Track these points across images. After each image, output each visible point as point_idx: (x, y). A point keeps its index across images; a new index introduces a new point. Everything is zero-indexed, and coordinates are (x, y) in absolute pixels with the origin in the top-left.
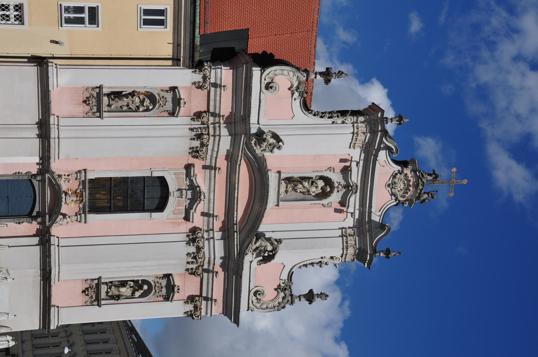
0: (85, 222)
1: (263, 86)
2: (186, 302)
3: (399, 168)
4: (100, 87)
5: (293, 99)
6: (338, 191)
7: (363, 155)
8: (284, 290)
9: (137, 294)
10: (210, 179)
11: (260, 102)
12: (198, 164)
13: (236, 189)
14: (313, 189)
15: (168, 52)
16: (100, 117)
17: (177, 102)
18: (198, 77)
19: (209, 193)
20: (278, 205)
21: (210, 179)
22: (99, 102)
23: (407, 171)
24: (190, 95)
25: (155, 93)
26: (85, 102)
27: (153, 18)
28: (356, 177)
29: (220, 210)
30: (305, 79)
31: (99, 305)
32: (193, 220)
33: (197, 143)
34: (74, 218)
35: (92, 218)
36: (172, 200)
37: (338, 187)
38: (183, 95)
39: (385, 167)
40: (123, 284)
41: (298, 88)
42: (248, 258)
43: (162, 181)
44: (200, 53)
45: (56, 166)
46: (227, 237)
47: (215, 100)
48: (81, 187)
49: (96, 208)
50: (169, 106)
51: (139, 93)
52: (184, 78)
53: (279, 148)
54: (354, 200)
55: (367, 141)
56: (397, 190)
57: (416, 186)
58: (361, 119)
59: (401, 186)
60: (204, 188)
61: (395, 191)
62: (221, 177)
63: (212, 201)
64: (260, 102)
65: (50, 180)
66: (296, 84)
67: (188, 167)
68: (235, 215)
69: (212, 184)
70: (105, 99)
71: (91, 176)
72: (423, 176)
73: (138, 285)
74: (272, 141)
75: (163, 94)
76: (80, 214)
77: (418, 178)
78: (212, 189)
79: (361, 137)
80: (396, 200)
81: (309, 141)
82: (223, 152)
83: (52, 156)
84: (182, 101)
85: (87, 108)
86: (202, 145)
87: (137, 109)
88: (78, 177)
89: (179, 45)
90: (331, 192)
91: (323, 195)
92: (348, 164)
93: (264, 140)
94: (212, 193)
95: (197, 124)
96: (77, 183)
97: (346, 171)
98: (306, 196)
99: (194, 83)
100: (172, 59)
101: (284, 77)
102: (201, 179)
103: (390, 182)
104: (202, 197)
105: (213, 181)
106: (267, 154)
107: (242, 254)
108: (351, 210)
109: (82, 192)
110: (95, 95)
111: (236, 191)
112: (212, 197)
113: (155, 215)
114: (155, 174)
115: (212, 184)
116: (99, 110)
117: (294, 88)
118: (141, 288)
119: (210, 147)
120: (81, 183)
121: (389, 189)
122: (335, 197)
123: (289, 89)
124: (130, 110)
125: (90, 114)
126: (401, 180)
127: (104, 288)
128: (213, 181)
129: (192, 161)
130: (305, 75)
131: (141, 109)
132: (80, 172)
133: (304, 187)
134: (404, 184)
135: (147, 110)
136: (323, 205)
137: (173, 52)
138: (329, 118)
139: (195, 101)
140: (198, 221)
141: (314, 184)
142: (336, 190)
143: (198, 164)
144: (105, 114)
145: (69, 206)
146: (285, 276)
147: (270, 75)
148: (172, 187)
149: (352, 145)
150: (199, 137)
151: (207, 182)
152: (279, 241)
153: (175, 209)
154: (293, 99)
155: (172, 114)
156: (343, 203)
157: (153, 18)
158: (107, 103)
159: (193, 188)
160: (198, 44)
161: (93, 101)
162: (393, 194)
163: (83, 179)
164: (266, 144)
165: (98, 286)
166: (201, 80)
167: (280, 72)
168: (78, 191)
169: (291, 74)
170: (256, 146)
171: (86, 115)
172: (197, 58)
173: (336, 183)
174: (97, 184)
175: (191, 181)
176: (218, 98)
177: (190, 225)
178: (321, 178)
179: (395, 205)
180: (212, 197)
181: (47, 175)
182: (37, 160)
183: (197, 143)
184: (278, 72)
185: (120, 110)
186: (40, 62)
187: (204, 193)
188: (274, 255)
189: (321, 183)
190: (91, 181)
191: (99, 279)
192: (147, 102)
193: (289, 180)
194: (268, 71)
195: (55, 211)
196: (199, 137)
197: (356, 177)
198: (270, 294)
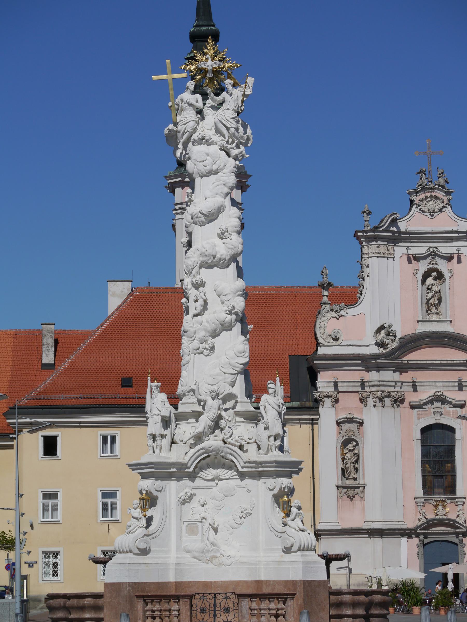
0: (465, 498)
1: (335, 343)
3: (414, 207)
4: (338, 487)
5: (347, 315)
6: (437, 264)
7: (400, 244)
10: (424, 386)
11: (350, 346)
12: (412, 397)
13: (432, 362)
15: (306, 428)
16: (364, 487)
17: (350, 420)
18: (328, 402)
19: (437, 386)
20: (451, 321)
21: (424, 386)
22: (351, 489)
23: (417, 199)
26: (351, 500)
29: (453, 376)
30: (328, 306)
32: (462, 401)
33: (388, 401)
34: (460, 507)
35: (459, 492)
36: (444, 421)
37: (433, 265)
38: (343, 415)
39: (414, 222)
41: (336, 312)
43: (424, 431)
44: (307, 401)
45: (411, 524)
47: (348, 386)
48: (431, 501)
49: (451, 489)
50: (354, 427)
51: (342, 454)
52: (328, 415)
53: (390, 326)
54: (445, 248)
55: (386, 243)
56: (436, 208)
57: (432, 189)
58: (365, 250)
59: (431, 205)
61: (437, 209)
63: (445, 384)
64: (350, 346)
65: (424, 528)
66: (333, 314)
68: (458, 362)
69: (428, 384)
71: (419, 492)
72: (421, 185)
74: (383, 333)
75: (343, 433)
76: (457, 502)
77: (424, 189)
78: (433, 384)
79: (383, 249)
80: (446, 207)
81: (388, 296)
82: (396, 376)
83: (399, 527)
84: (348, 416)
86: (389, 396)
87: (358, 455)
88: (422, 504)
89: (300, 420)
92: (411, 256)
93: (382, 341)
94: (437, 384)
95: (370, 401)
96: (427, 505)
97: (417, 258)
99: (333, 406)
100: (312, 425)
101: (327, 325)
102: (424, 395)
103: (428, 214)
104: (439, 394)
105: (426, 384)
106: (398, 336)
109: (436, 501)
110: (345, 491)
111: (434, 362)
112: (441, 384)
113: (458, 435)
114: (418, 436)
115: (428, 384)
116: (358, 487)
117: (336, 315)
119: (391, 389)
120: (427, 501)
121: (435, 214)
122: (442, 266)
123: (338, 319)
124: (357, 461)
125: (362, 495)
126: (425, 204)
128: (426, 384)
130: (324, 306)
131: (356, 452)
132: (416, 503)
133: (432, 297)
134: (429, 201)
135: (357, 444)
136: (450, 278)
137: (306, 424)
138: (364, 280)
139: (350, 404)
141: (430, 287)
142: (436, 267)
143: (412, 397)
144: (362, 483)
145: (451, 512)
147: (324, 337)
148: (431, 421)
151: (426, 389)
153: (453, 417)
154: (347, 315)
155: (361, 424)
156: (449, 258)
158: (352, 481)
160: (298, 403)
161: (351, 492)
162: (441, 210)
163: (423, 500)
164: (385, 340)
166: (330, 399)
167: (322, 331)
168: (435, 504)
169: (323, 319)
170: (388, 348)
172: (311, 404)
173: (428, 267)
174: (428, 488)
175: (425, 404)
176: (345, 384)
178: (424, 281)
179: (451, 207)
180: (441, 384)
181: (419, 531)
182: (404, 539)
183: (388, 401)
184: (322, 331)
187: (436, 392)
189: (430, 281)
190: (424, 494)
192: (350, 446)
193: (428, 310)
194: (321, 340)
195: (452, 524)
196: (381, 400)
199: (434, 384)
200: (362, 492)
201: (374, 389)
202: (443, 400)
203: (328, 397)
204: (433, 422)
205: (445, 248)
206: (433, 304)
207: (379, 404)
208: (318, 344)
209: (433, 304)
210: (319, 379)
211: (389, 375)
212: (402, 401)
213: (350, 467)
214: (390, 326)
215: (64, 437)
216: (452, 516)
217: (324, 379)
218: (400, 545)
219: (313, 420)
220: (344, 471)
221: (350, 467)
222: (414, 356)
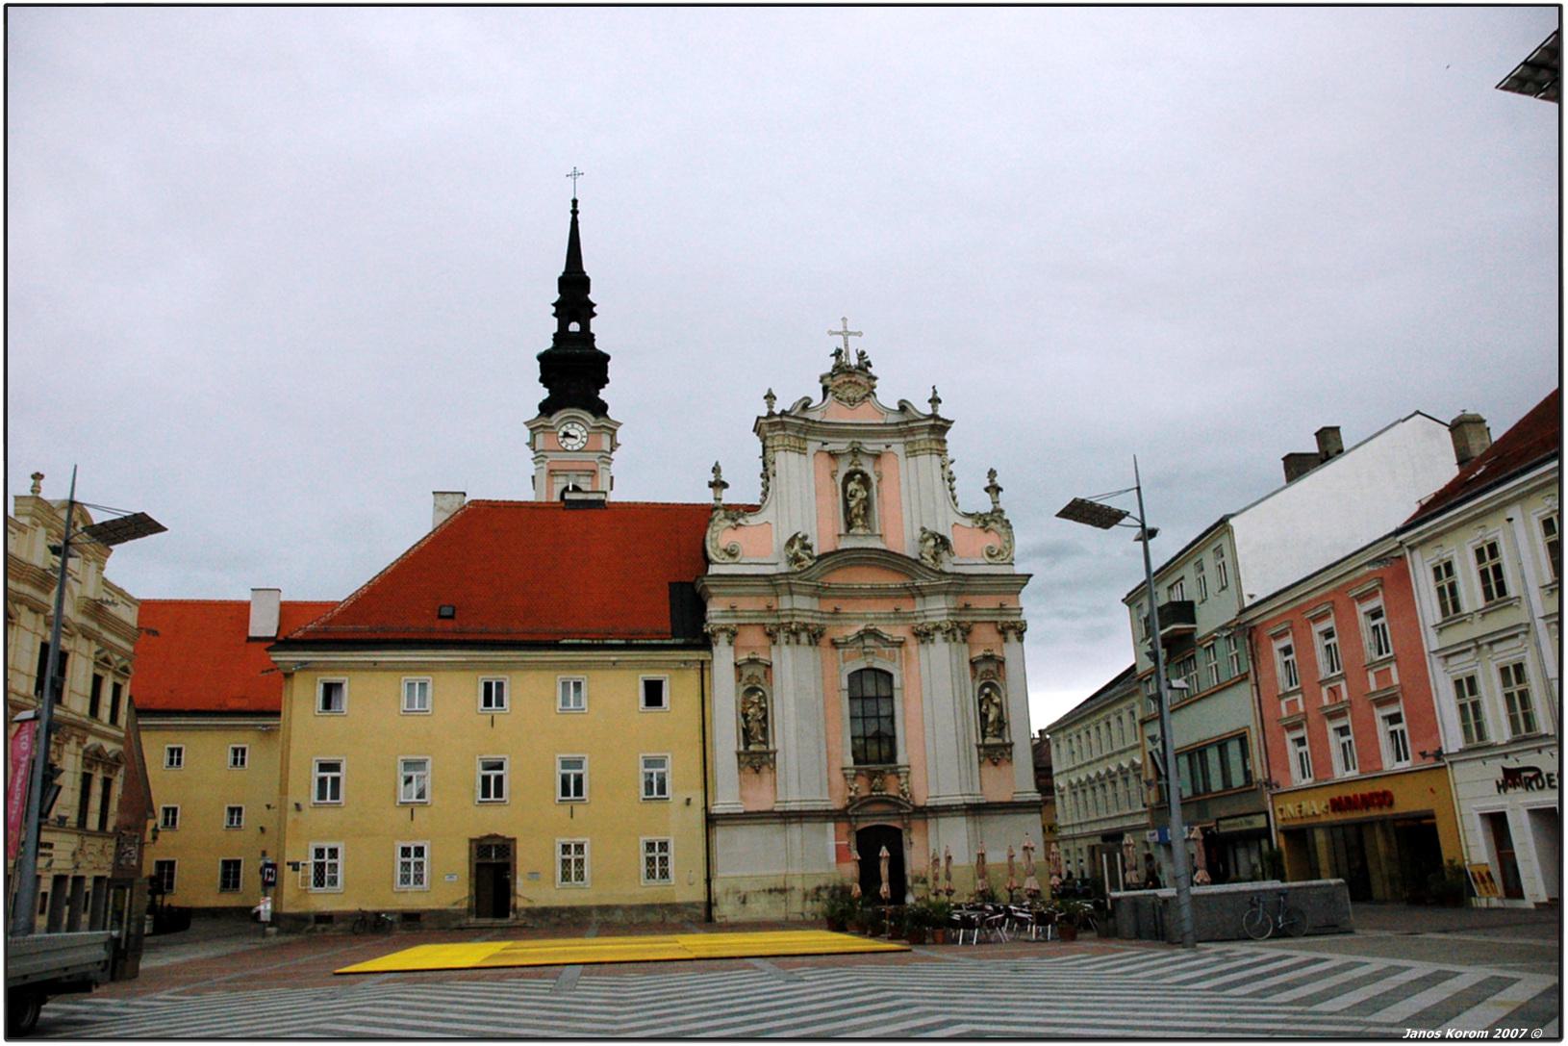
2: (1006, 640)
4: (739, 754)
8: (986, 523)
9: (996, 700)
14: (859, 495)
17: (752, 662)
18: (723, 638)
22: (756, 756)
24: (747, 648)
25: (743, 689)
27: (653, 694)
28: (841, 445)
29: (885, 607)
31: (1011, 745)
33: (804, 638)
35: (901, 759)
36: (876, 665)
38: (743, 657)
40: (984, 717)
42: (947, 568)
43: (856, 677)
45: (837, 804)
46: (919, 593)
50: (759, 672)
52: (723, 658)
53: (805, 537)
54: (870, 445)
59: (850, 393)
60: (861, 627)
62: (848, 608)
66: (729, 523)
67: (834, 644)
70: (752, 748)
71: (849, 761)
73: (984, 700)
74: (797, 547)
85: (765, 769)
87: (765, 710)
90: (862, 473)
91: (865, 481)
95: (782, 636)
98: (867, 505)
102: (852, 632)
107: (942, 573)
108: (883, 448)
114: (845, 683)
116: (767, 753)
118: (988, 696)
122: (867, 467)
124: (765, 718)
127: (990, 740)
129: (825, 641)
139: (753, 638)
140: (899, 632)
146: (968, 522)
149: (802, 451)
150: (795, 633)
152: (923, 530)
155: (769, 667)
157: (653, 694)
159: (861, 637)
165: (986, 747)
171: (774, 769)
177: (912, 641)
183: (804, 638)
185: (764, 731)
186: (711, 821)
188: (943, 538)
189: (852, 486)
190: (856, 762)
191: (978, 747)
193: (849, 525)
194: (711, 555)
196: (795, 633)
197: (841, 445)
198: (992, 540)
199: (862, 618)
200: (774, 761)
201: (785, 620)
202: (874, 634)
203: (721, 630)
204: (863, 665)
205: (870, 445)
206: (857, 512)
207: (792, 639)
208: (708, 561)
209: (857, 512)
210: (710, 608)
211: (802, 603)
212: (821, 634)
213: (755, 729)
214: (805, 537)
215: (352, 687)
216: (892, 792)
217: (716, 611)
218: (825, 833)
219: (702, 662)
220: (746, 732)
221: (755, 729)
222: (838, 578)
